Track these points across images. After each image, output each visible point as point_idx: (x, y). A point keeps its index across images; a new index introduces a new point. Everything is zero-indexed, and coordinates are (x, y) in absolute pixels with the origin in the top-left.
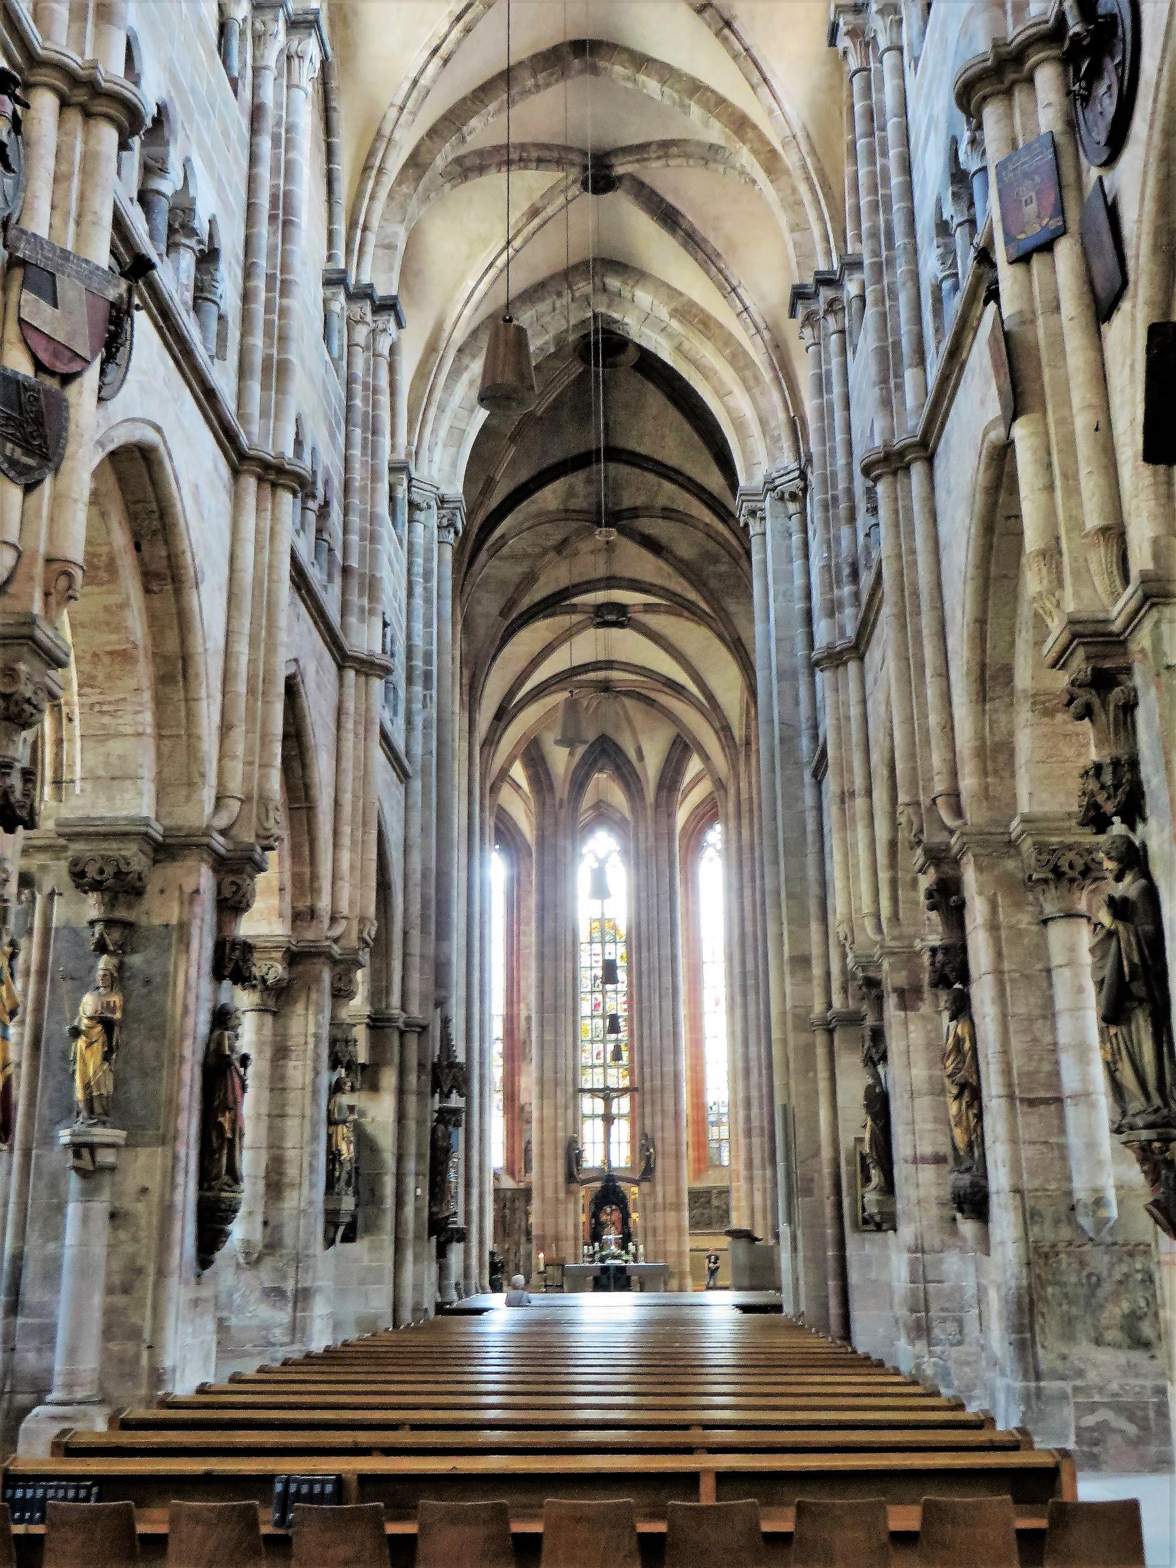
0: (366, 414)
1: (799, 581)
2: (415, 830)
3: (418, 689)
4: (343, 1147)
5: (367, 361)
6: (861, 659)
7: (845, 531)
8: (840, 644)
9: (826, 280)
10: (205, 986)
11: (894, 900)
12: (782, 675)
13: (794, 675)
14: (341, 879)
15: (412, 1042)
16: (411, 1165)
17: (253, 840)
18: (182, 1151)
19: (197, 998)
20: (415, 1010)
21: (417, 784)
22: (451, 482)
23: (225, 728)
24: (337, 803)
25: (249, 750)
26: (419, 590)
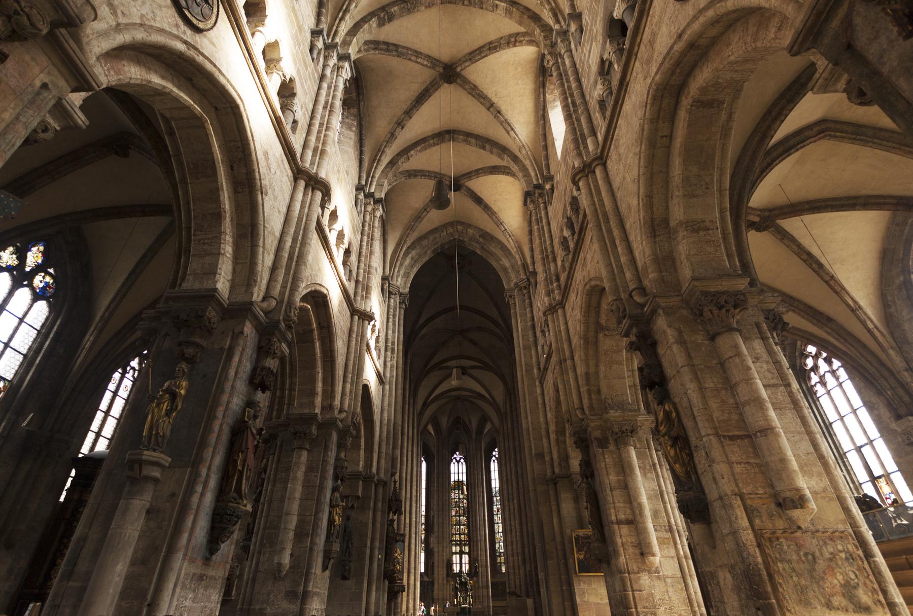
0: (369, 234)
1: (529, 315)
2: (386, 403)
3: (389, 353)
4: (337, 518)
5: (371, 218)
6: (564, 308)
7: (552, 265)
8: (554, 303)
9: (538, 187)
10: (241, 386)
11: (590, 398)
12: (524, 348)
13: (530, 348)
14: (345, 395)
15: (381, 490)
16: (377, 544)
17: (281, 318)
18: (204, 472)
19: (233, 387)
20: (382, 475)
21: (387, 387)
22: (404, 289)
23: (274, 268)
24: (346, 365)
25: (285, 282)
26: (391, 320)
